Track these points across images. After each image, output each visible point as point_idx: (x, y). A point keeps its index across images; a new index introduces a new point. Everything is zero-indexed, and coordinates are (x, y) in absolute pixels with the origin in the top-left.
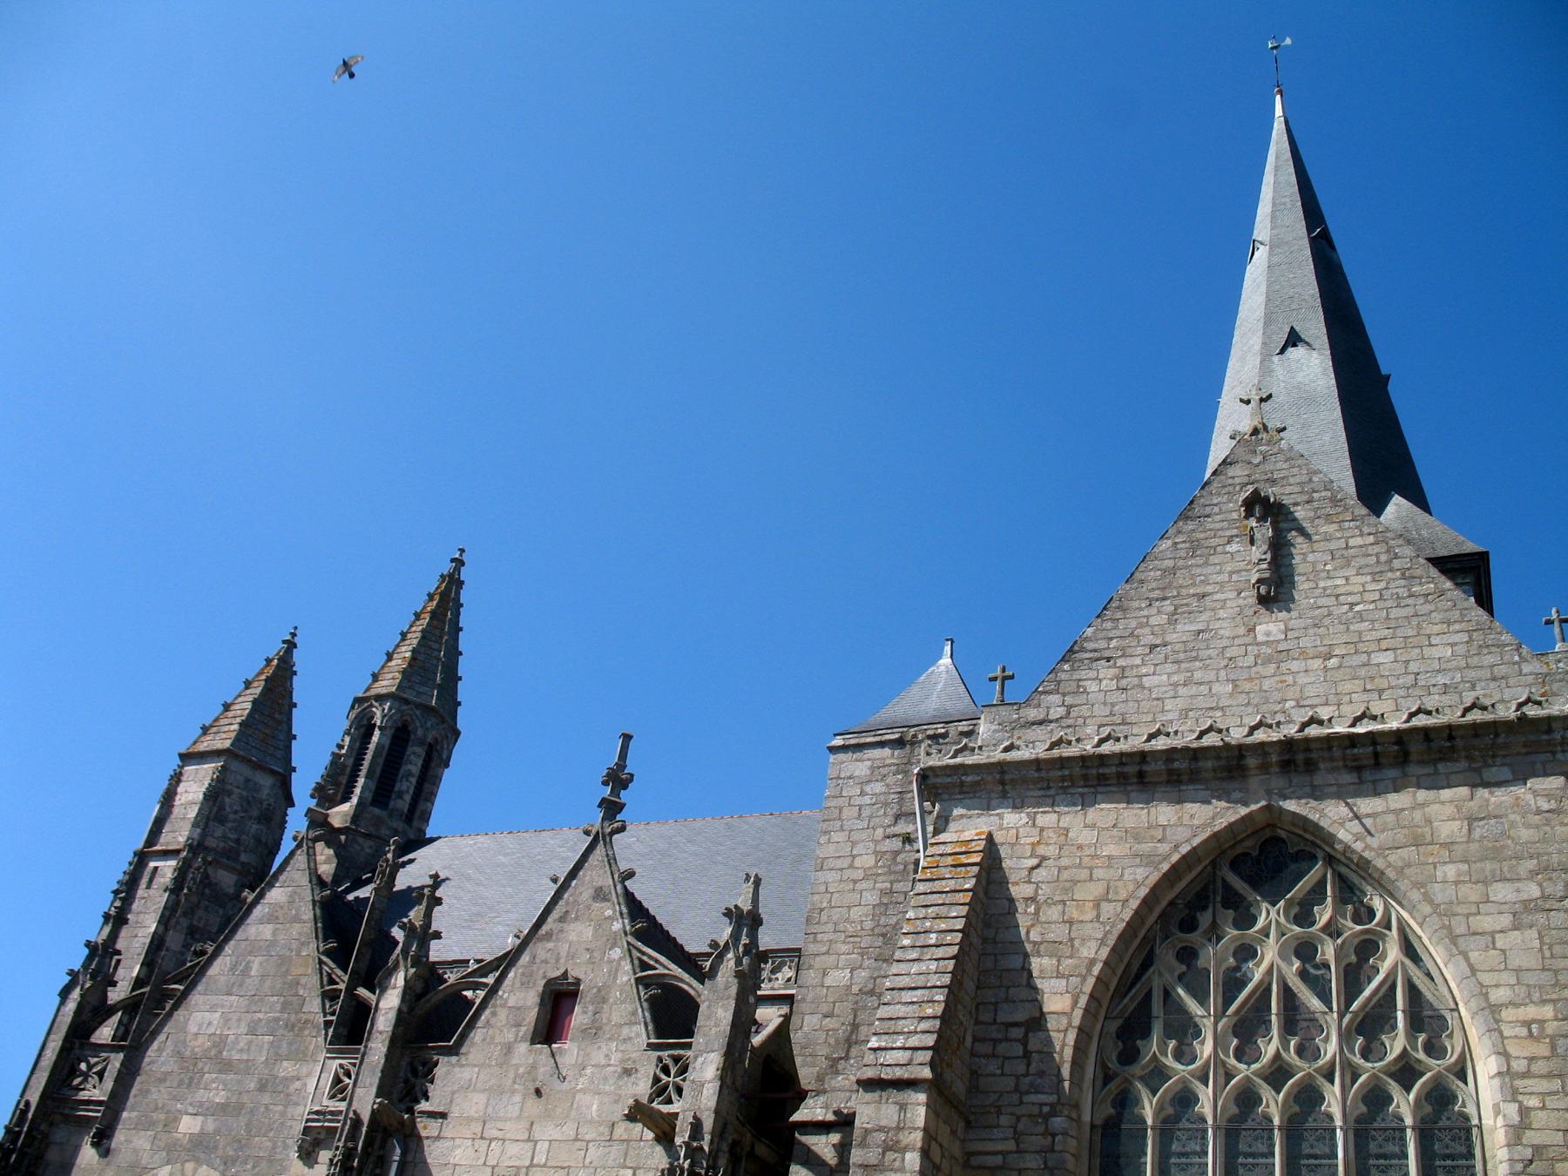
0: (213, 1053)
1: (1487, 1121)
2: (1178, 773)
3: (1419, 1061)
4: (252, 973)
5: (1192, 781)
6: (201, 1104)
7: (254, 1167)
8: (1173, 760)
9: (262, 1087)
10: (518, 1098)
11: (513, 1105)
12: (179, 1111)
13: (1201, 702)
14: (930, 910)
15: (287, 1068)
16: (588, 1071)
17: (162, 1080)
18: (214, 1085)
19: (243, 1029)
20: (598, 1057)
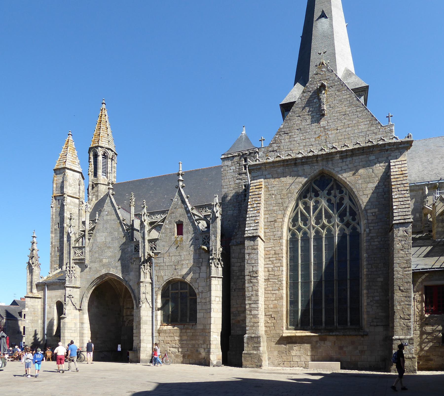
1: (362, 232)
2: (304, 162)
3: (350, 222)
5: (307, 164)
8: (302, 160)
12: (102, 258)
13: (308, 144)
14: (254, 199)
18: (108, 252)
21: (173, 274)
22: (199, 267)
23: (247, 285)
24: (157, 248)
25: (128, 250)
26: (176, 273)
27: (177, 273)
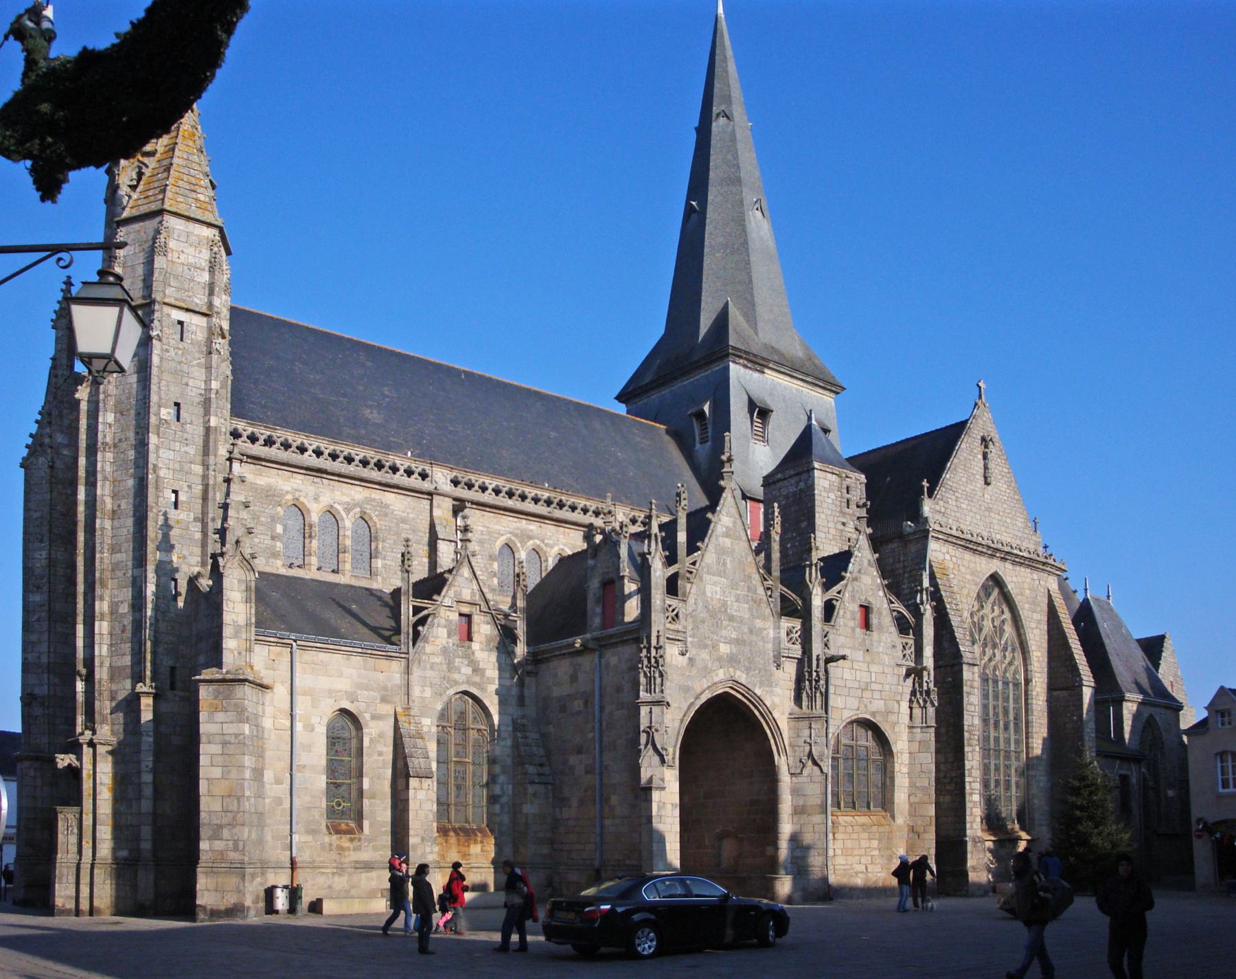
0: (723, 610)
4: (728, 566)
6: (726, 638)
7: (759, 672)
9: (751, 632)
10: (861, 653)
11: (860, 655)
15: (759, 623)
16: (882, 644)
17: (703, 622)
19: (733, 599)
20: (883, 638)
21: (858, 709)
22: (898, 702)
23: (967, 749)
24: (831, 644)
25: (768, 633)
26: (863, 706)
27: (866, 706)
